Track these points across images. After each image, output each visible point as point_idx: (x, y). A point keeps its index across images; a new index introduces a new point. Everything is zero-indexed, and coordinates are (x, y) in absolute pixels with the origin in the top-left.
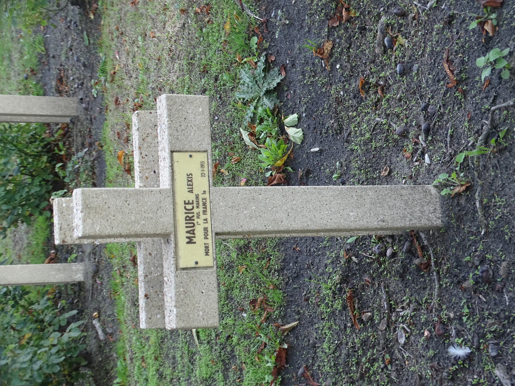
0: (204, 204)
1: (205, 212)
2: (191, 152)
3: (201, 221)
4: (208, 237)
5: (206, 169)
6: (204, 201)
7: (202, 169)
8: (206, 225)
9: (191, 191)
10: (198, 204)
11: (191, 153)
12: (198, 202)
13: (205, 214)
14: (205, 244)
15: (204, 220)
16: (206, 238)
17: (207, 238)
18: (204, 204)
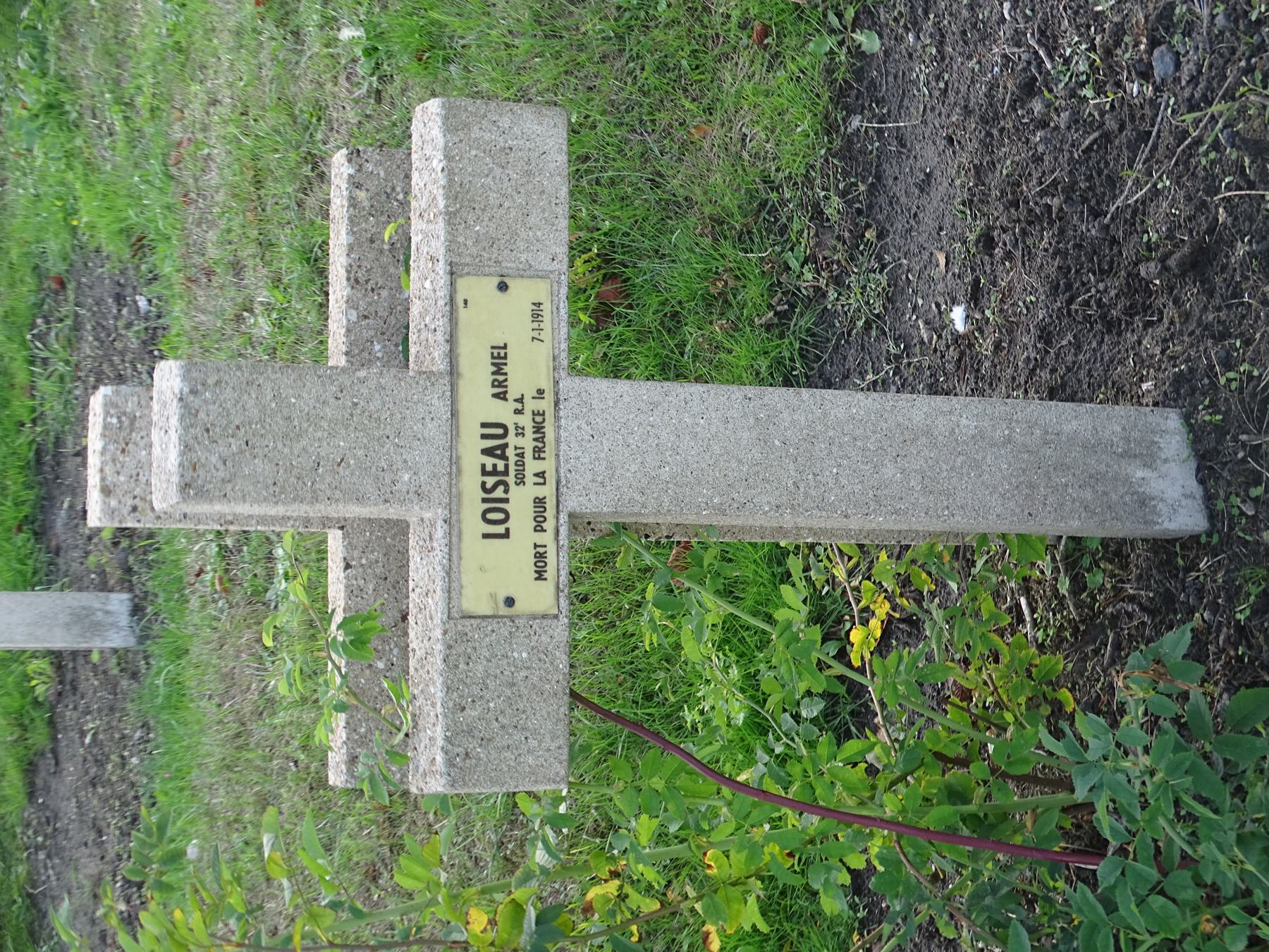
0: (539, 429)
1: (538, 453)
4: (544, 525)
5: (547, 325)
6: (539, 419)
9: (502, 396)
13: (539, 458)
14: (536, 546)
15: (536, 475)
16: (539, 529)
18: (539, 429)
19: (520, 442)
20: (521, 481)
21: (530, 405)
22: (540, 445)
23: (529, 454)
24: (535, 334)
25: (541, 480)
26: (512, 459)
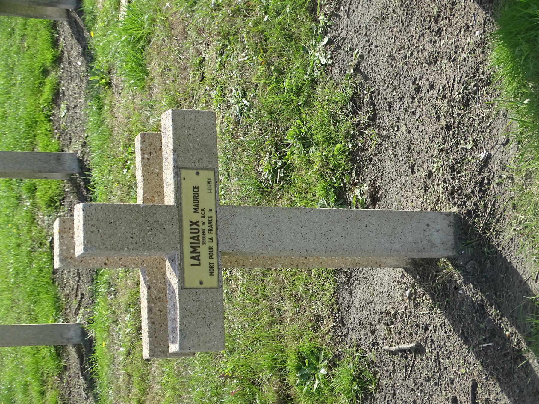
0: (210, 223)
1: (210, 231)
4: (213, 256)
6: (210, 219)
7: (209, 186)
8: (211, 245)
14: (210, 264)
15: (209, 239)
16: (211, 257)
17: (212, 258)
18: (210, 223)
19: (203, 227)
20: (204, 243)
21: (207, 214)
23: (207, 231)
24: (209, 191)
26: (200, 234)
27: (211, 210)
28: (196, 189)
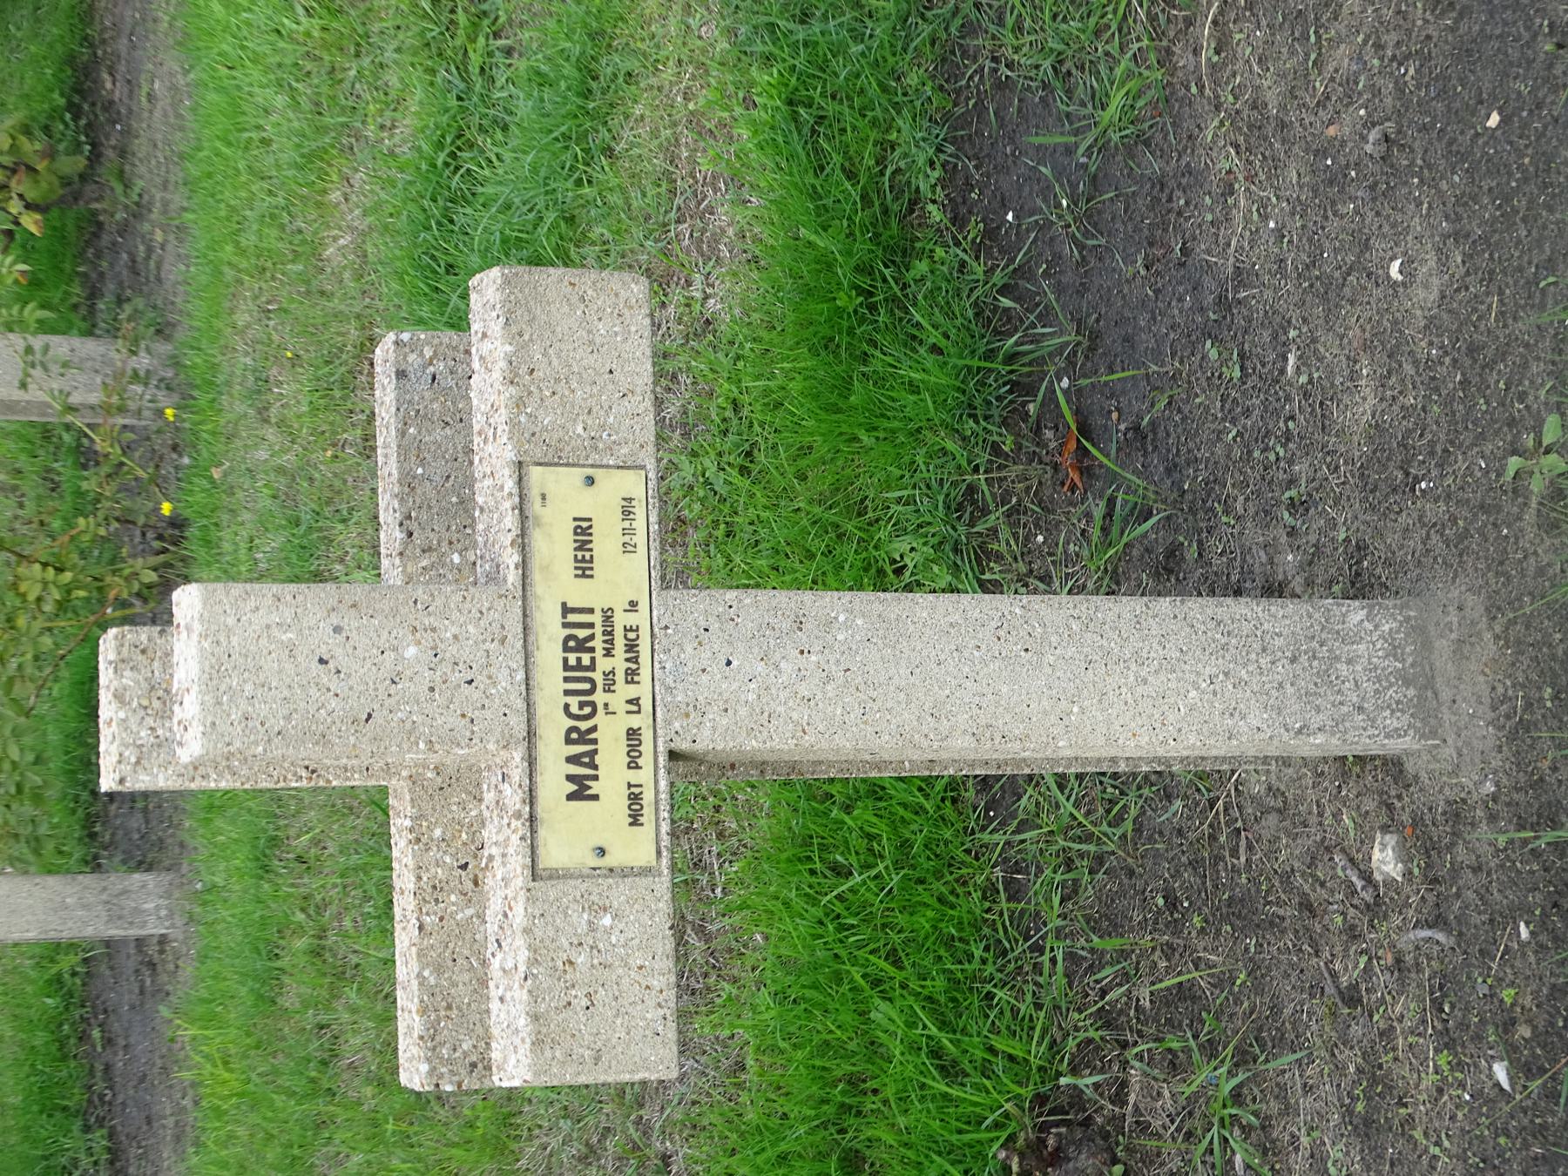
0: (631, 647)
2: (590, 463)
3: (618, 700)
4: (640, 761)
5: (640, 524)
6: (632, 635)
8: (635, 721)
10: (611, 642)
11: (590, 471)
12: (611, 633)
13: (633, 682)
14: (630, 786)
15: (629, 702)
16: (633, 765)
17: (638, 767)
18: (631, 647)
21: (621, 620)
22: (634, 666)
23: (620, 676)
25: (635, 708)
27: (633, 604)
28: (583, 532)
